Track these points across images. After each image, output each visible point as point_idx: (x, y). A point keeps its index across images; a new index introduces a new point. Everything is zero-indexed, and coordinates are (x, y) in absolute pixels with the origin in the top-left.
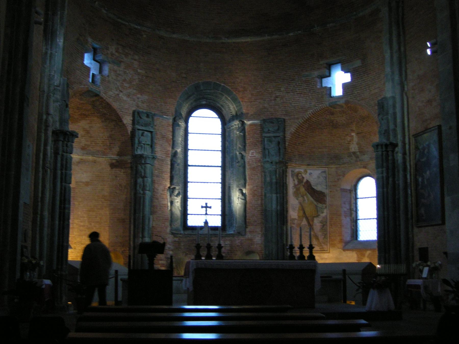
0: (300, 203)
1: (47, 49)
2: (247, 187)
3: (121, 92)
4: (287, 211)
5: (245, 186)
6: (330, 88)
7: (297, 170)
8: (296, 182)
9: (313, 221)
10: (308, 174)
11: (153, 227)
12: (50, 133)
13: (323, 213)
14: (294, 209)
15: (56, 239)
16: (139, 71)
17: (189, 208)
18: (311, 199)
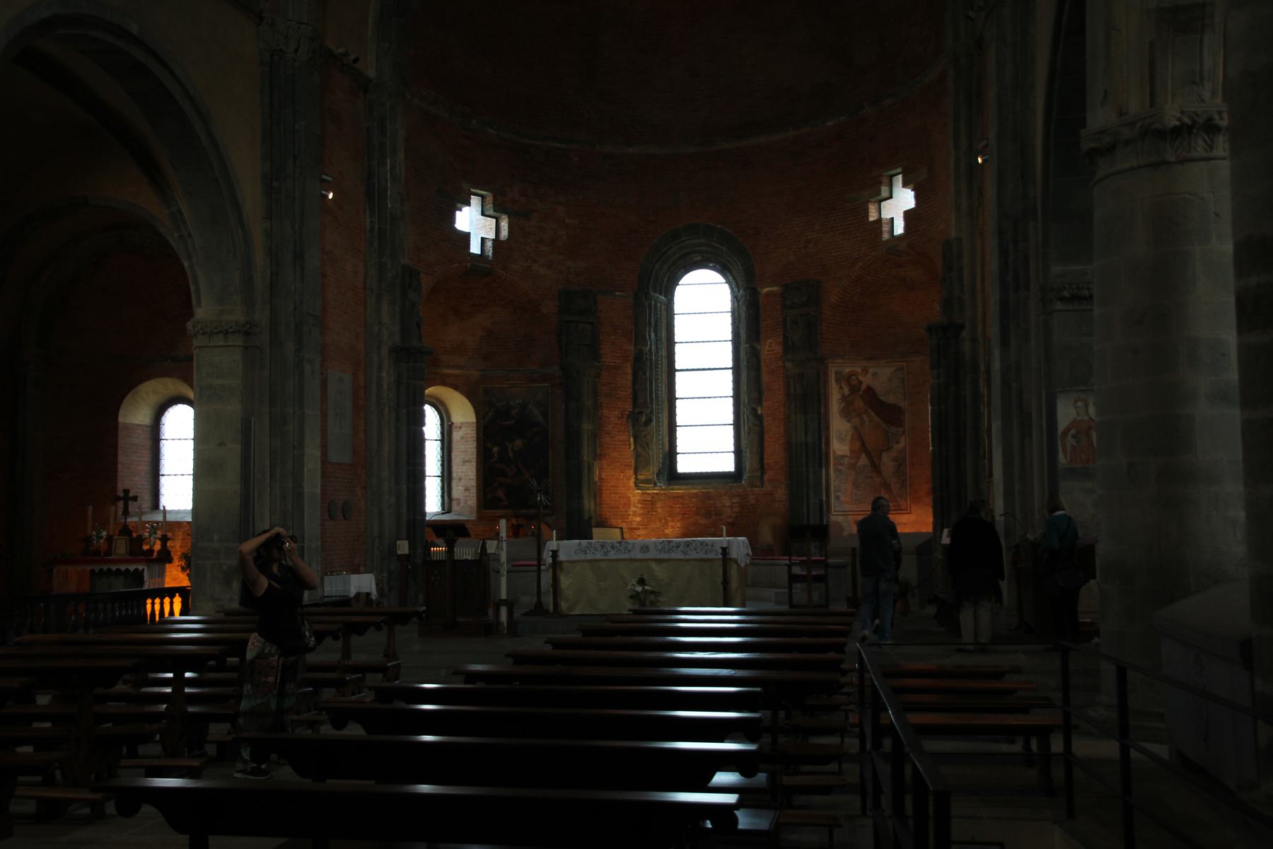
0: (855, 428)
1: (372, 222)
2: (765, 404)
3: (536, 261)
4: (828, 444)
5: (760, 402)
6: (892, 219)
7: (847, 370)
8: (846, 391)
9: (880, 458)
10: (870, 375)
11: (601, 479)
12: (385, 351)
13: (898, 442)
14: (841, 440)
15: (404, 509)
17: (679, 442)
18: (877, 419)
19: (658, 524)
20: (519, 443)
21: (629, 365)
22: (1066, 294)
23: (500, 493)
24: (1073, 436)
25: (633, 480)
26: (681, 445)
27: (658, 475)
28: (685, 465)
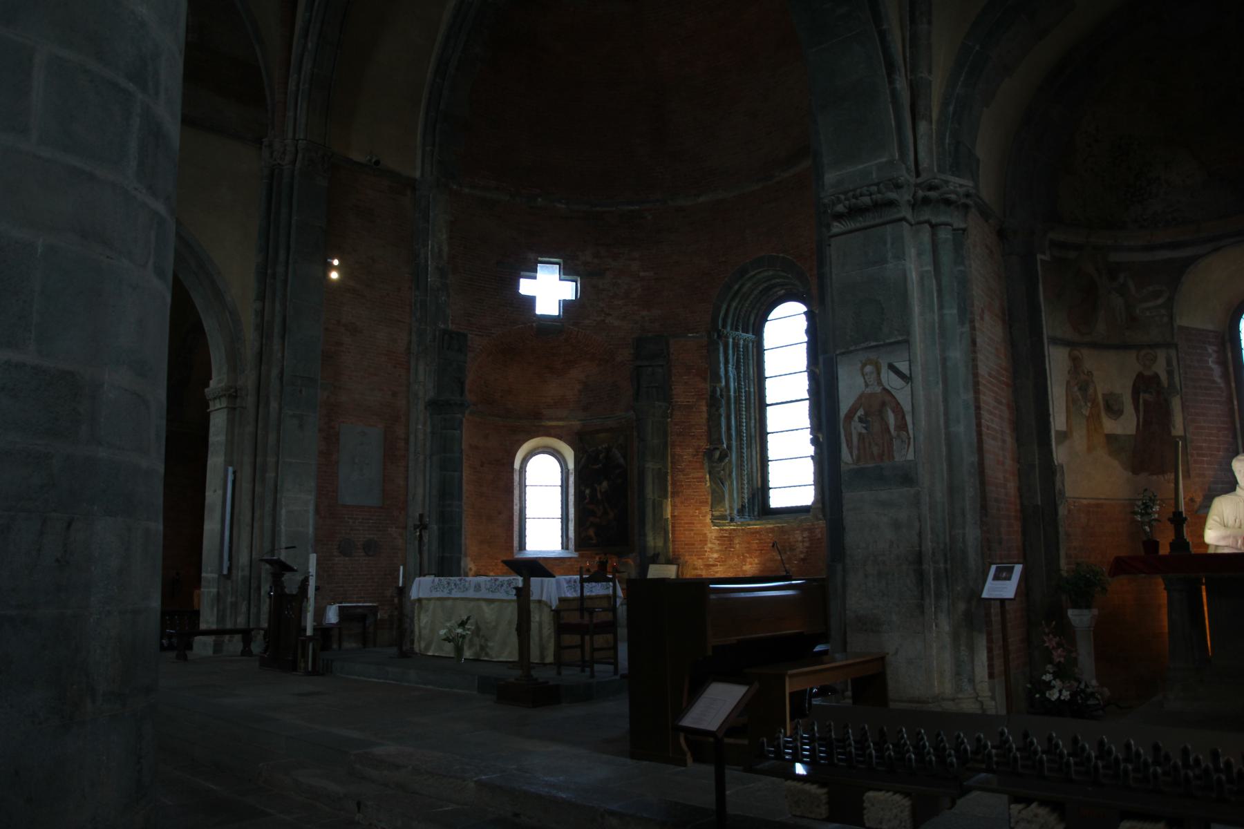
16: (642, 274)
19: (736, 561)
20: (605, 484)
21: (704, 403)
22: (840, 208)
23: (591, 532)
24: (861, 420)
25: (709, 516)
26: (773, 480)
27: (741, 511)
28: (777, 500)
